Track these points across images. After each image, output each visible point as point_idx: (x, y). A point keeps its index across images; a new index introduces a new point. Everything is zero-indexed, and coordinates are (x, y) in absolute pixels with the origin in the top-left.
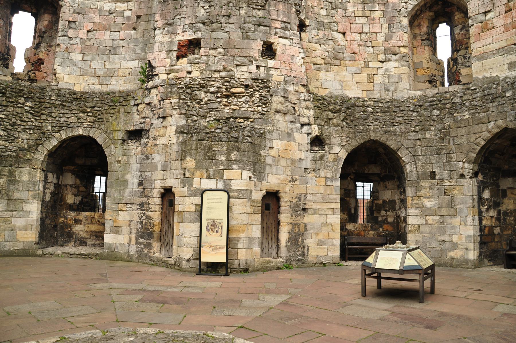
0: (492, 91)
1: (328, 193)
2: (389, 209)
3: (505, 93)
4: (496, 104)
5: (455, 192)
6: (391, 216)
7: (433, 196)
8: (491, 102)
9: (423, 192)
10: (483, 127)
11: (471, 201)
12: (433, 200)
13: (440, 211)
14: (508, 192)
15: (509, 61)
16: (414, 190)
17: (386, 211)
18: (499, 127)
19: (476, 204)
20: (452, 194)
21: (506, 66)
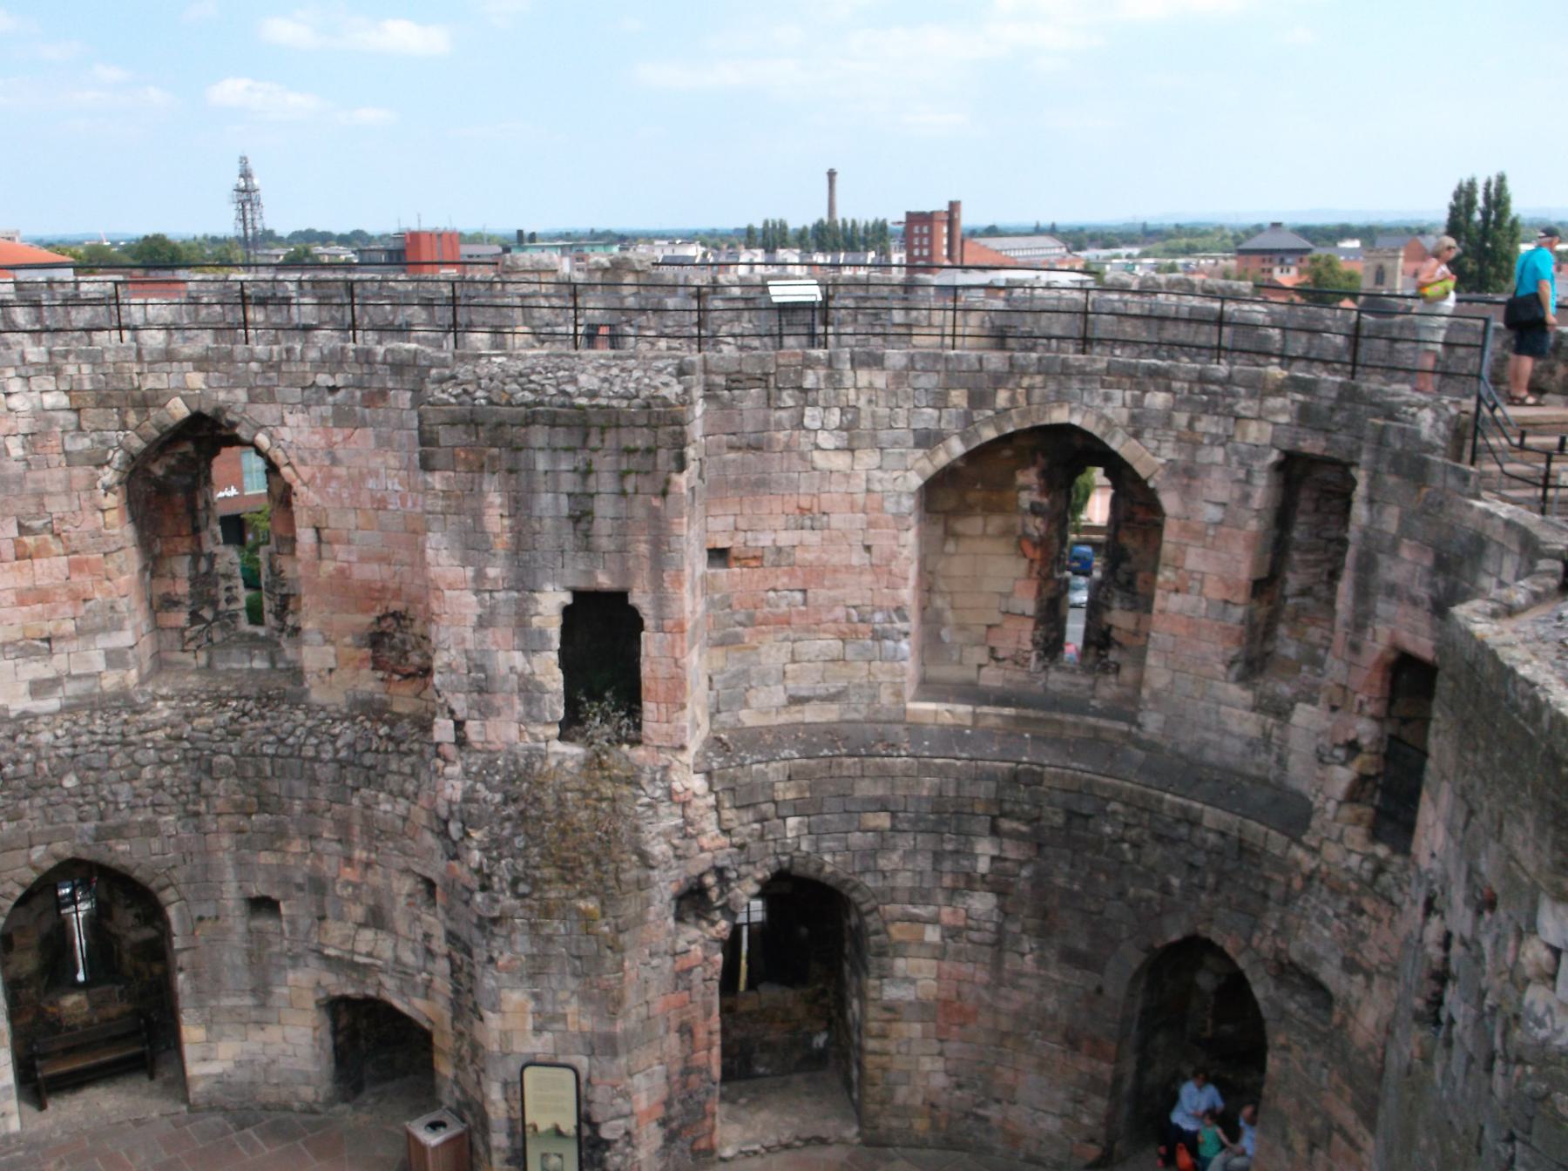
0: (25, 769)
3: (61, 778)
4: (38, 801)
8: (26, 798)
10: (19, 857)
15: (30, 677)
18: (56, 856)
21: (24, 687)
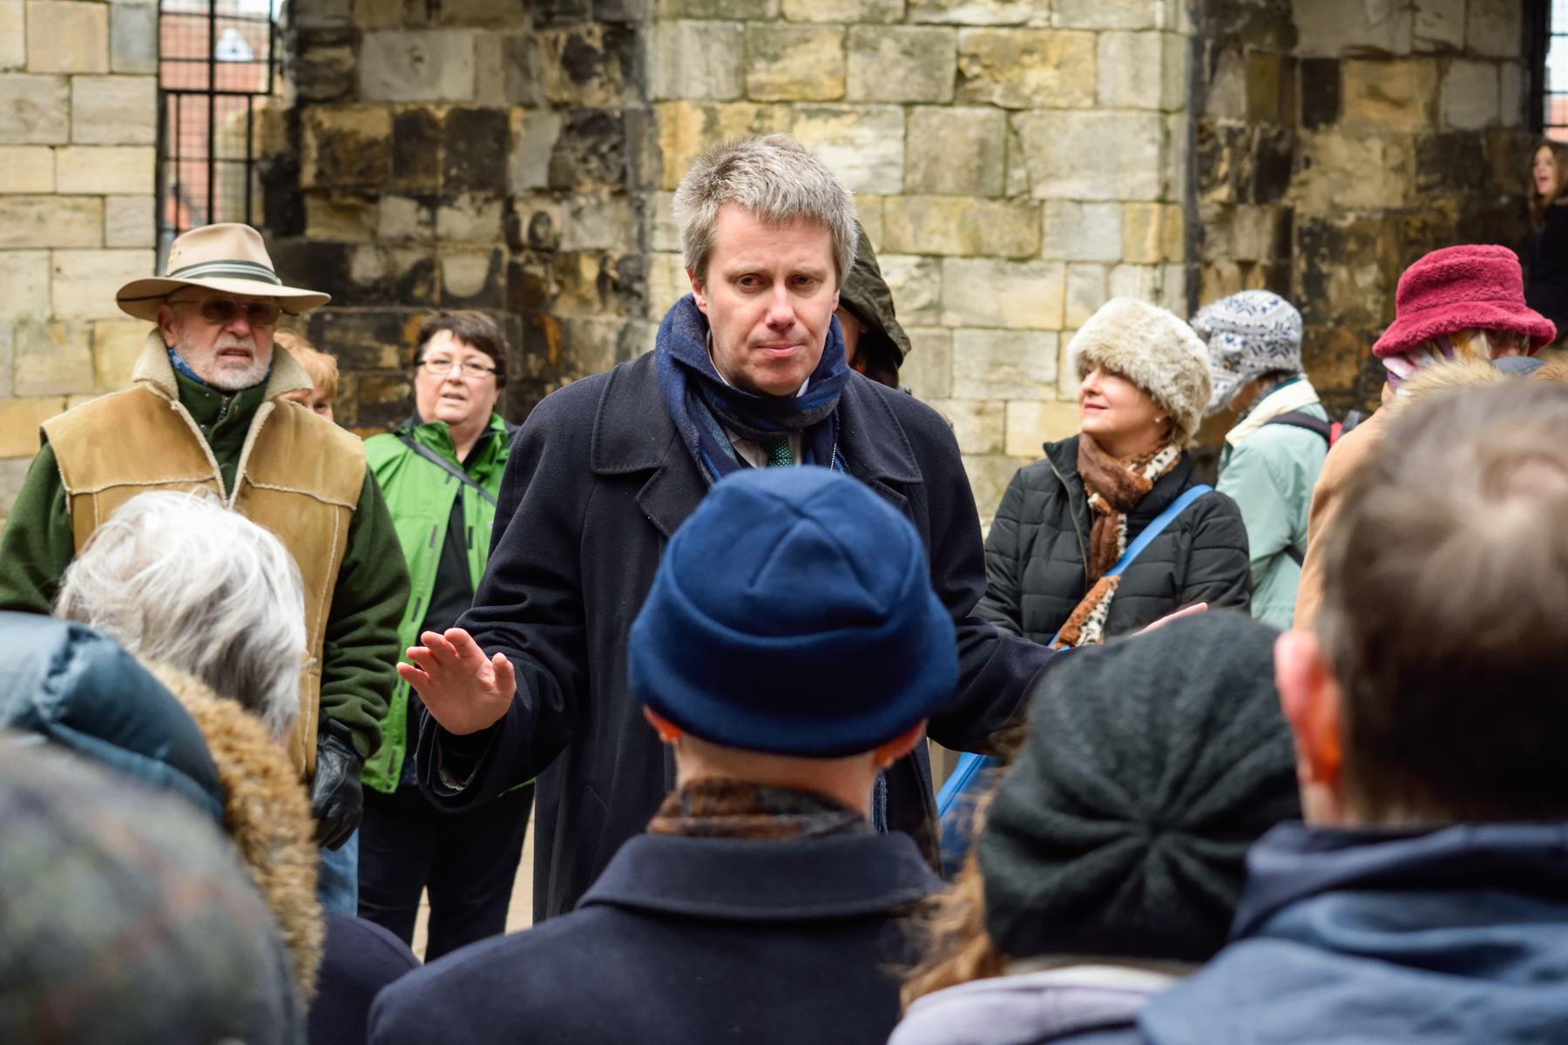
1: (67, 64)
2: (455, 186)
5: (1037, 76)
6: (466, 246)
7: (869, 108)
9: (797, 64)
11: (1152, 151)
12: (865, 133)
13: (917, 218)
14: (1353, 81)
16: (721, 56)
17: (430, 202)
19: (1177, 173)
20: (1013, 90)
